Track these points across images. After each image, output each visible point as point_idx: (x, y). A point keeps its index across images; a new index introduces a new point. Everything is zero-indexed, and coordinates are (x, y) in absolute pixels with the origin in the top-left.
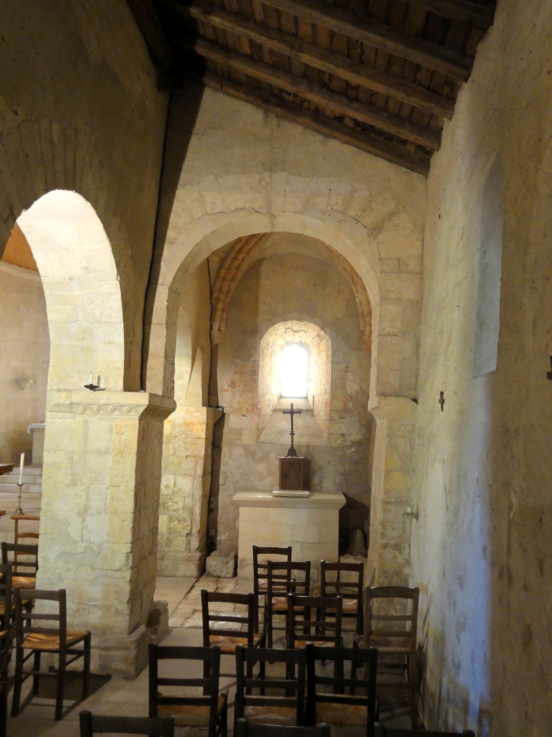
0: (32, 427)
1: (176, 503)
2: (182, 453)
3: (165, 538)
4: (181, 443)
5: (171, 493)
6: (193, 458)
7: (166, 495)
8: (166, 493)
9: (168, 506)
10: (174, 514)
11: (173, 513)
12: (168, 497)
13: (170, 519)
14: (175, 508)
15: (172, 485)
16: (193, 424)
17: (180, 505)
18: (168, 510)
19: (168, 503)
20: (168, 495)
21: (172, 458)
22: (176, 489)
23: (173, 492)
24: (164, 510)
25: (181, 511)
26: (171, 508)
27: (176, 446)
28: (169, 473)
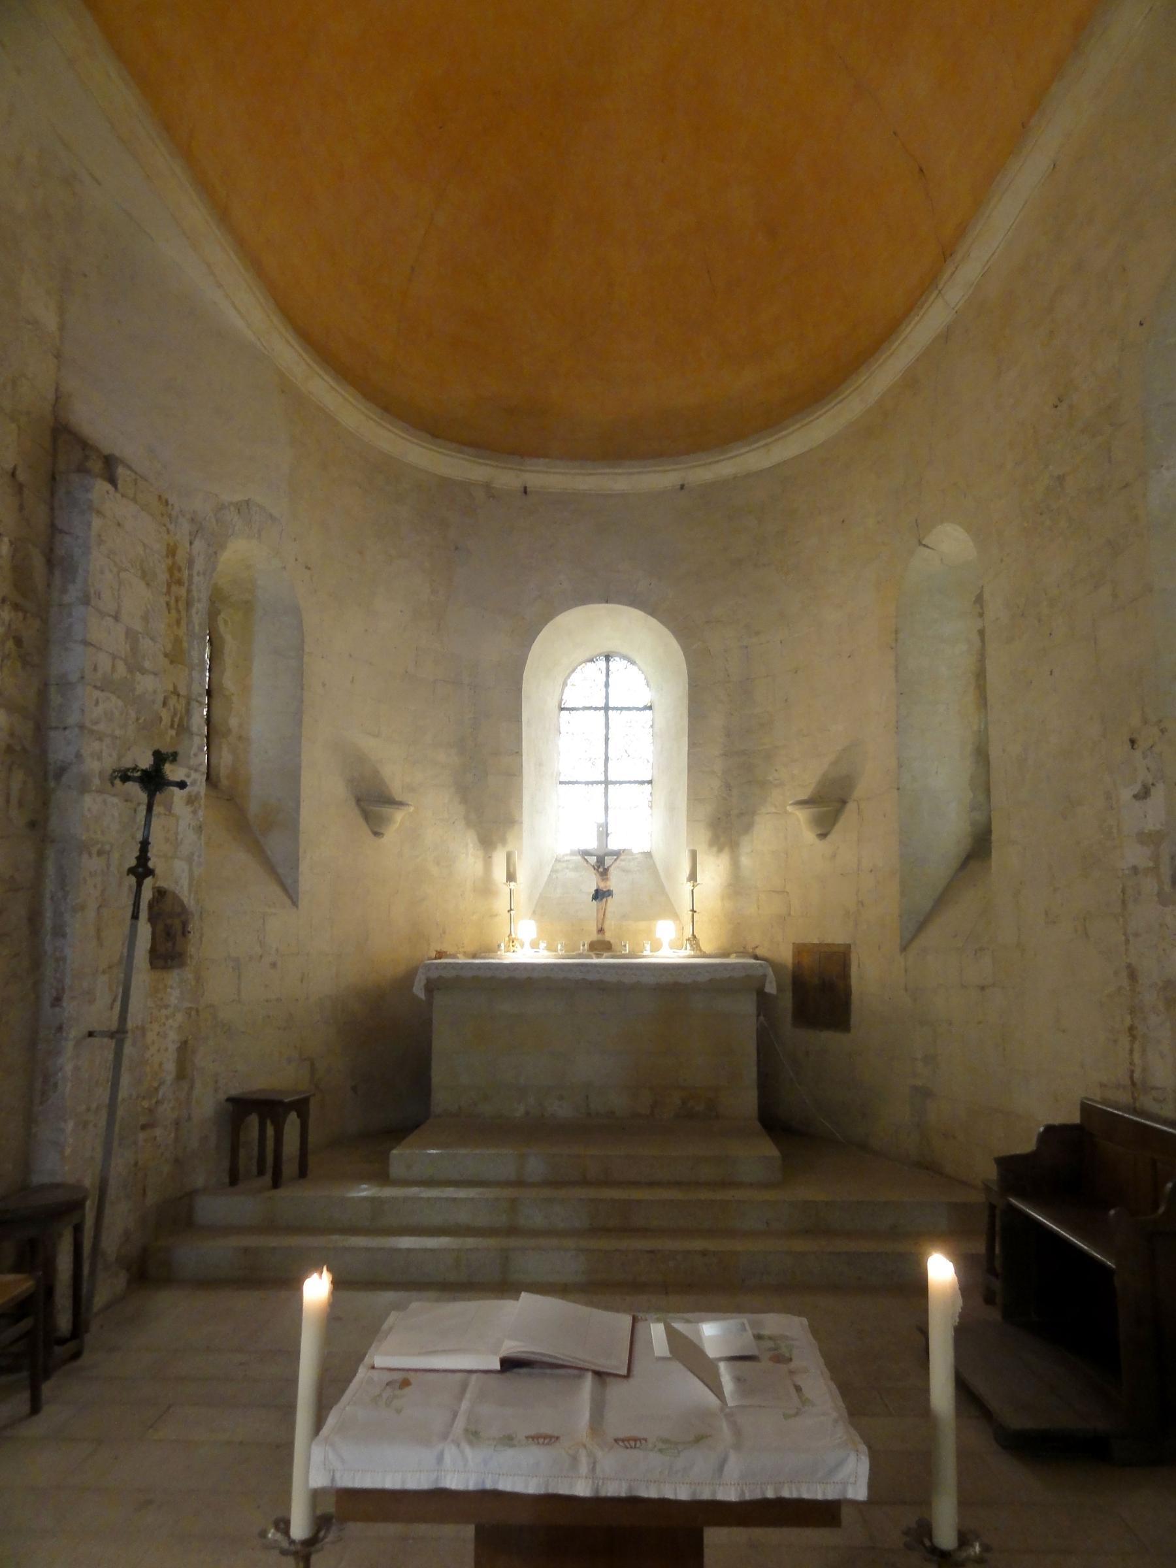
0: (434, 975)
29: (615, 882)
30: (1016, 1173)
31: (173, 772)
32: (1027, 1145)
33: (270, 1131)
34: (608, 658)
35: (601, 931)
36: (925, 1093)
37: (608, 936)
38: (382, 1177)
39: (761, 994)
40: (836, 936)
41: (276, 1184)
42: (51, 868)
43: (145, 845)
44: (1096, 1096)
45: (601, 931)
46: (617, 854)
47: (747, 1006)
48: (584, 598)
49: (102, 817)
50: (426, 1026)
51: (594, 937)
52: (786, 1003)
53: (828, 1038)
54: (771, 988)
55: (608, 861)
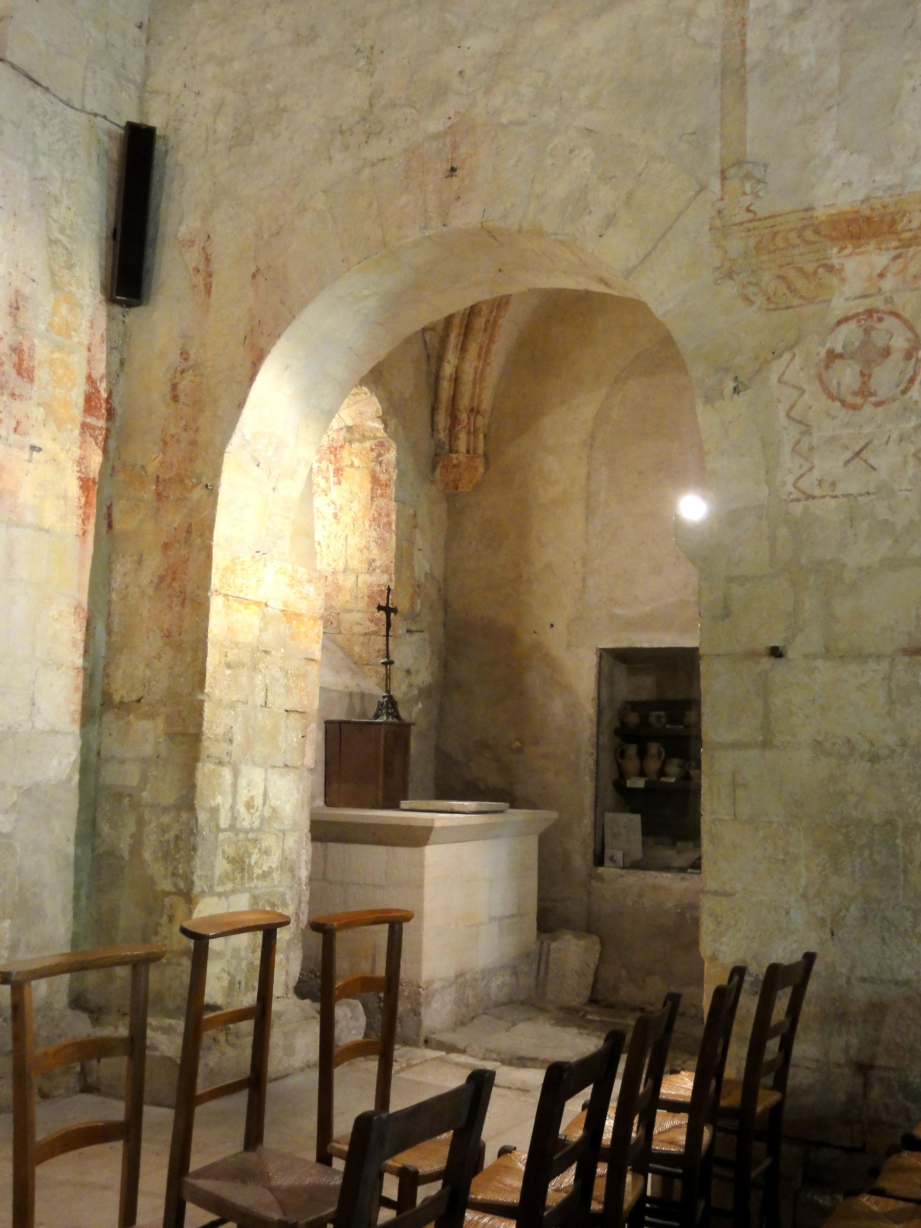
1: (267, 852)
2: (280, 702)
3: (244, 964)
4: (279, 675)
5: (257, 824)
6: (298, 716)
7: (247, 832)
8: (246, 824)
9: (249, 864)
11: (260, 883)
12: (251, 836)
14: (265, 868)
16: (298, 615)
17: (274, 860)
18: (251, 878)
19: (250, 856)
20: (252, 829)
21: (260, 716)
23: (262, 820)
24: (242, 878)
25: (276, 875)
26: (257, 871)
27: (268, 682)
28: (254, 764)
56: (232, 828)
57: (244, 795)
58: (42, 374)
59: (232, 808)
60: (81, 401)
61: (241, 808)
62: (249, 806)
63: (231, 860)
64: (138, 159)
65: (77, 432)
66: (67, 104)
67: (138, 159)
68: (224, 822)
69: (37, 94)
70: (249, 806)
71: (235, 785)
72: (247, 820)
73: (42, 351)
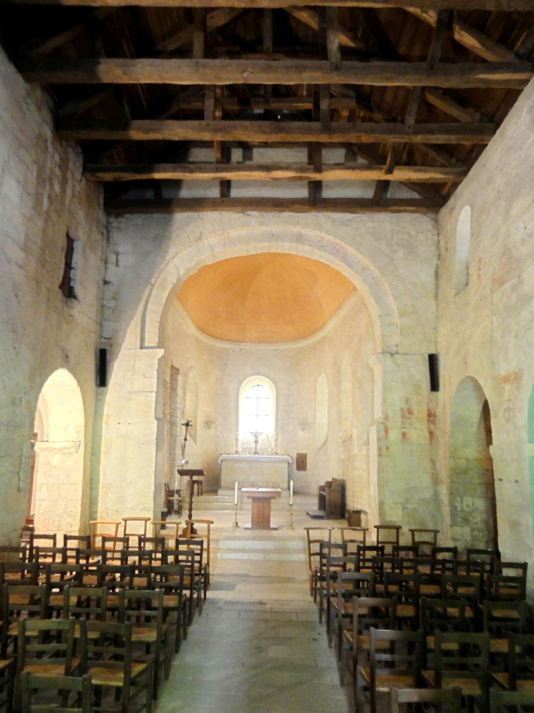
1: (476, 518)
4: (475, 475)
5: (470, 511)
10: (475, 526)
13: (472, 530)
15: (470, 504)
22: (474, 508)
29: (260, 439)
30: (322, 488)
31: (190, 424)
32: (323, 484)
33: (200, 486)
34: (258, 386)
35: (256, 450)
36: (317, 481)
37: (257, 451)
38: (217, 495)
39: (289, 463)
40: (304, 452)
41: (198, 495)
42: (172, 439)
43: (186, 435)
44: (335, 477)
45: (256, 450)
46: (260, 433)
47: (286, 465)
48: (253, 374)
49: (181, 431)
50: (220, 469)
51: (254, 451)
52: (295, 466)
53: (302, 473)
54: (290, 462)
55: (258, 434)
56: (462, 511)
57: (465, 503)
58: (415, 412)
59: (462, 506)
60: (426, 415)
61: (464, 506)
62: (467, 506)
63: (463, 519)
64: (433, 360)
65: (426, 422)
66: (416, 355)
67: (433, 360)
68: (459, 509)
69: (407, 357)
70: (467, 506)
71: (462, 500)
72: (466, 509)
73: (415, 408)
